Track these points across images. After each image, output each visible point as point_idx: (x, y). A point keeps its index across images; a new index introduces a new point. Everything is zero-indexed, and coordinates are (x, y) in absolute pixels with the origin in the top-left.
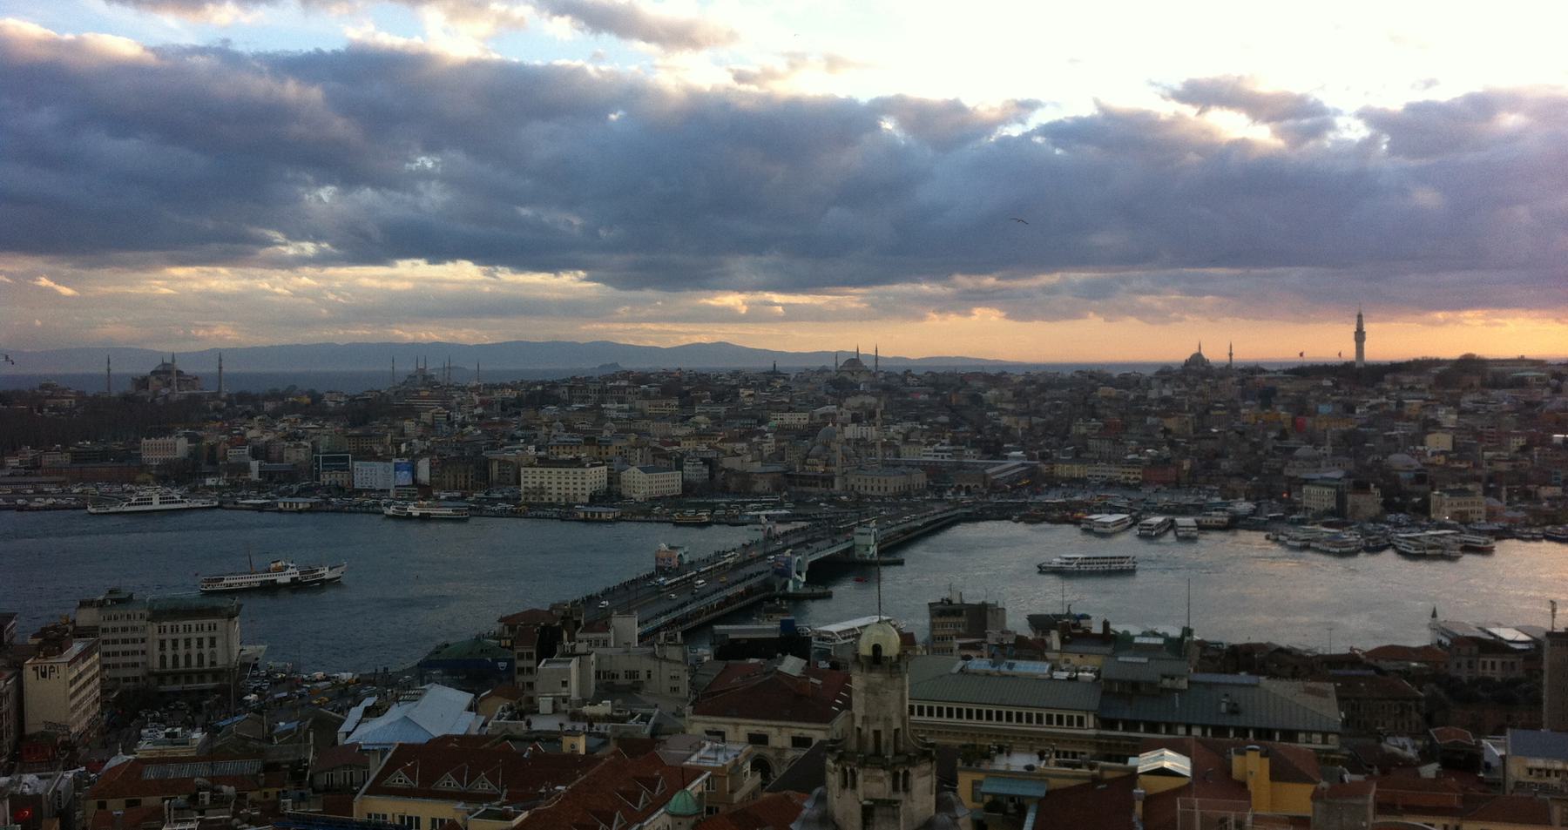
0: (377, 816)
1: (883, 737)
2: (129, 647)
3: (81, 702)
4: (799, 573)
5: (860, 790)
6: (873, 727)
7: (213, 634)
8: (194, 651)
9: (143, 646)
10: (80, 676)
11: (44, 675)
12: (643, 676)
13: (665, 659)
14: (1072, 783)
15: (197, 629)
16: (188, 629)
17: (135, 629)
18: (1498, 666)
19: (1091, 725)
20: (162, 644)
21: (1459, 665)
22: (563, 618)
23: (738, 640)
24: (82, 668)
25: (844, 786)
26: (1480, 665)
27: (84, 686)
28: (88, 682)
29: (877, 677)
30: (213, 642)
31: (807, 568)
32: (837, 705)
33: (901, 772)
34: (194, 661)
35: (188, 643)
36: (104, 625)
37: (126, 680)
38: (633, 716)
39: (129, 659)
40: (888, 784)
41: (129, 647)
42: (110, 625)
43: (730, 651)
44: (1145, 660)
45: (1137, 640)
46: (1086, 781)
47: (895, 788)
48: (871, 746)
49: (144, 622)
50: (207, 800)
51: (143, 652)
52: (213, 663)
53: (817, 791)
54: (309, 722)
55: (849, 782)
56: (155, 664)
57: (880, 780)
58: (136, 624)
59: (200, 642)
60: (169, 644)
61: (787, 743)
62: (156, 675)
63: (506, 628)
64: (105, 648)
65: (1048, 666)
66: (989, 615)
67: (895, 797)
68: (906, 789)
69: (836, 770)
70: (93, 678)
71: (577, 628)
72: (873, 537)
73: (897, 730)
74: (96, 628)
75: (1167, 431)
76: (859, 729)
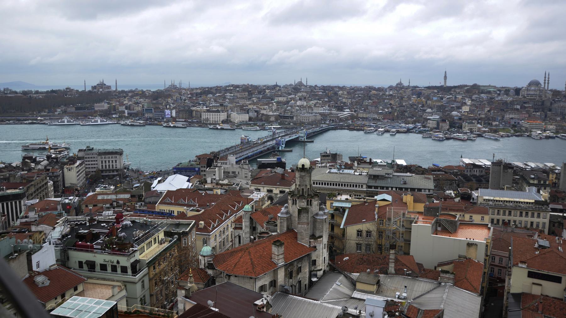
0: (162, 210)
1: (305, 190)
2: (93, 163)
3: (80, 178)
4: (283, 144)
5: (297, 205)
6: (302, 188)
7: (116, 159)
8: (111, 164)
9: (96, 163)
10: (79, 171)
11: (69, 170)
12: (237, 173)
13: (243, 168)
14: (359, 203)
16: (109, 158)
17: (94, 157)
18: (478, 171)
19: (365, 187)
20: (102, 162)
21: (467, 171)
22: (214, 156)
23: (265, 163)
24: (80, 168)
25: (293, 204)
26: (473, 171)
27: (81, 173)
28: (82, 172)
29: (303, 174)
30: (116, 161)
32: (293, 182)
33: (309, 200)
34: (111, 167)
35: (109, 161)
36: (85, 156)
37: (92, 172)
38: (234, 184)
39: (93, 166)
40: (306, 203)
41: (93, 163)
42: (87, 156)
43: (263, 166)
44: (381, 169)
45: (379, 164)
46: (361, 203)
47: (308, 205)
48: (301, 193)
49: (96, 156)
50: (115, 205)
51: (97, 164)
52: (116, 167)
53: (286, 205)
54: (143, 184)
55: (294, 203)
56: (101, 168)
57: (303, 202)
58: (94, 156)
59: (112, 161)
60: (104, 162)
61: (278, 192)
62: (101, 170)
63: (198, 159)
64: (86, 163)
65: (353, 171)
66: (338, 156)
67: (308, 207)
68: (311, 205)
69: (291, 199)
70: (83, 171)
71: (218, 159)
73: (309, 188)
74: (84, 157)
75: (391, 104)
76: (298, 188)
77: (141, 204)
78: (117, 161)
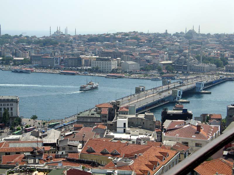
7: (12, 107)
15: (4, 105)
23: (170, 114)
30: (12, 109)
31: (182, 94)
61: (194, 145)
72: (201, 85)
77: (63, 153)
78: (13, 109)
